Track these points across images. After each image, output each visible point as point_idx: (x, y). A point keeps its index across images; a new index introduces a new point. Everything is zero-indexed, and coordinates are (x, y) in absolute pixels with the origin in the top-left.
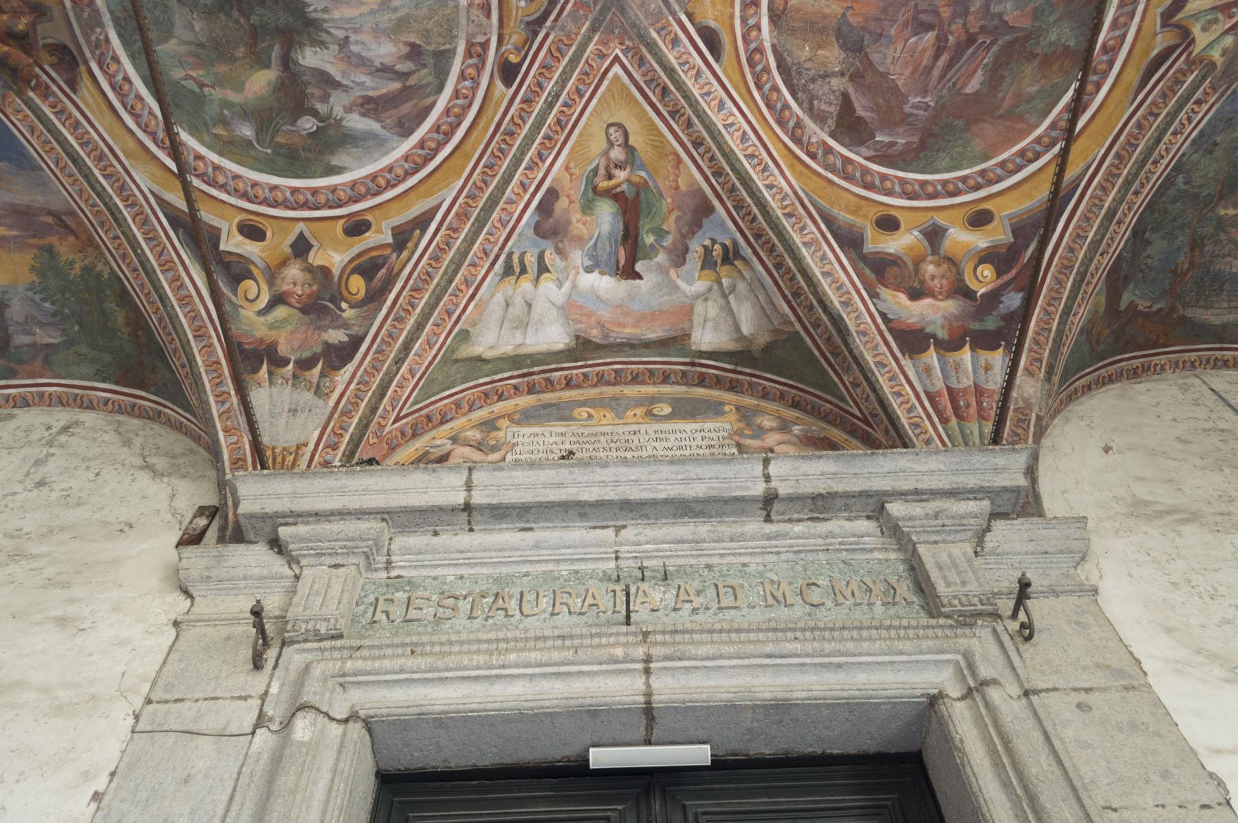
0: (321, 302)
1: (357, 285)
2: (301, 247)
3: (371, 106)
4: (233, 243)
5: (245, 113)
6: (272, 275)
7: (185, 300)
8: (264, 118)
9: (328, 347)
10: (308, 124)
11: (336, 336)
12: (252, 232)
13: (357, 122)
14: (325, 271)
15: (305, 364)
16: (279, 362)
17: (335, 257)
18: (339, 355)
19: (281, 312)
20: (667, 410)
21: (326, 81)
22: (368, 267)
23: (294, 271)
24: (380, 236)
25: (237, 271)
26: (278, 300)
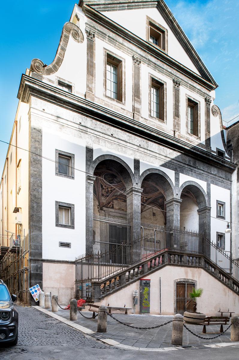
0: (107, 192)
1: (110, 192)
2: (108, 188)
3: (116, 182)
4: (104, 187)
5: (108, 180)
6: (105, 189)
7: (100, 190)
8: (110, 180)
9: (107, 196)
10: (112, 181)
11: (108, 195)
12: (105, 186)
13: (115, 182)
14: (108, 190)
15: (105, 196)
16: (104, 196)
17: (109, 190)
18: (108, 196)
19: (105, 192)
20: (123, 201)
21: (115, 180)
22: (111, 191)
23: (107, 190)
24: (113, 189)
25: (103, 189)
26: (105, 191)
